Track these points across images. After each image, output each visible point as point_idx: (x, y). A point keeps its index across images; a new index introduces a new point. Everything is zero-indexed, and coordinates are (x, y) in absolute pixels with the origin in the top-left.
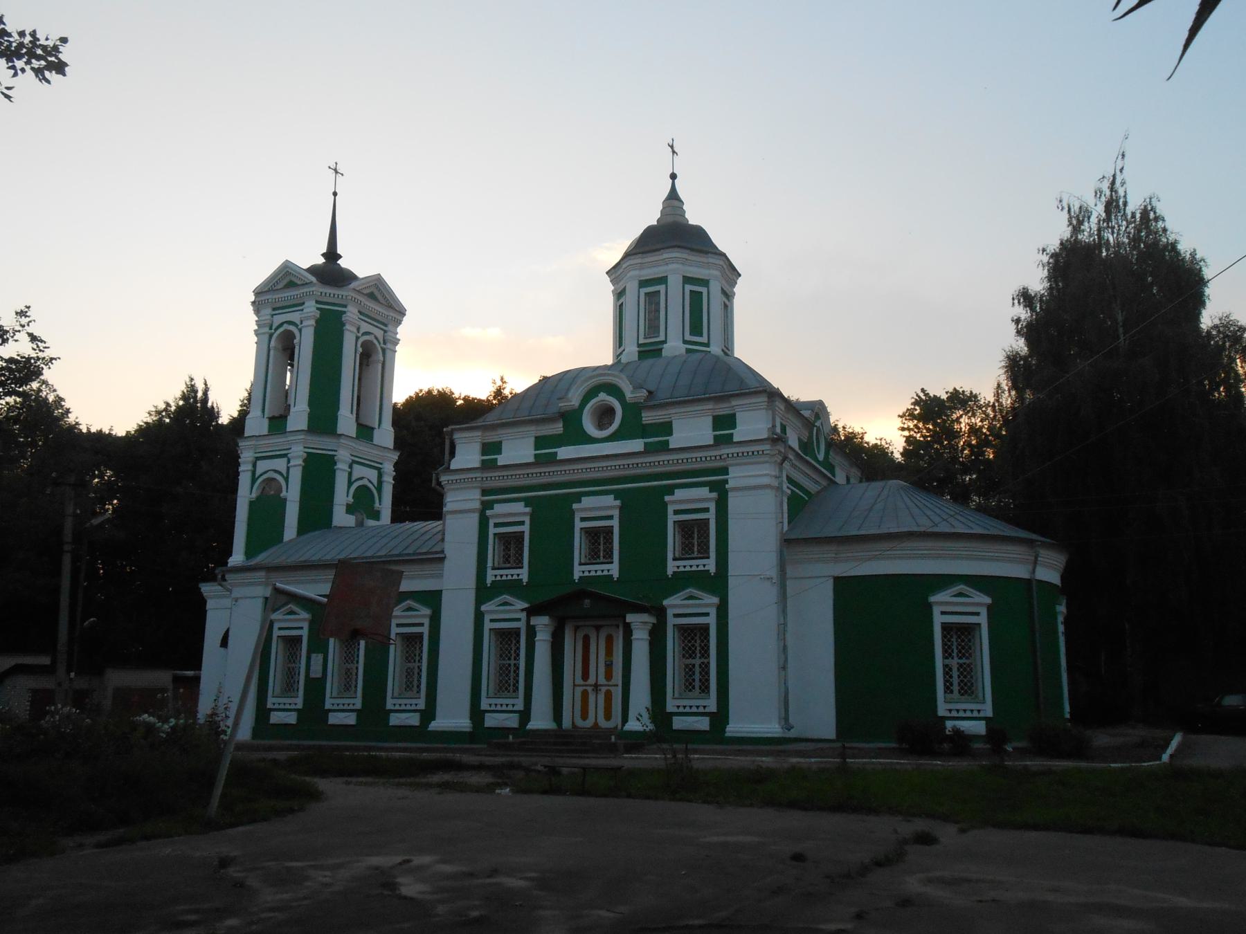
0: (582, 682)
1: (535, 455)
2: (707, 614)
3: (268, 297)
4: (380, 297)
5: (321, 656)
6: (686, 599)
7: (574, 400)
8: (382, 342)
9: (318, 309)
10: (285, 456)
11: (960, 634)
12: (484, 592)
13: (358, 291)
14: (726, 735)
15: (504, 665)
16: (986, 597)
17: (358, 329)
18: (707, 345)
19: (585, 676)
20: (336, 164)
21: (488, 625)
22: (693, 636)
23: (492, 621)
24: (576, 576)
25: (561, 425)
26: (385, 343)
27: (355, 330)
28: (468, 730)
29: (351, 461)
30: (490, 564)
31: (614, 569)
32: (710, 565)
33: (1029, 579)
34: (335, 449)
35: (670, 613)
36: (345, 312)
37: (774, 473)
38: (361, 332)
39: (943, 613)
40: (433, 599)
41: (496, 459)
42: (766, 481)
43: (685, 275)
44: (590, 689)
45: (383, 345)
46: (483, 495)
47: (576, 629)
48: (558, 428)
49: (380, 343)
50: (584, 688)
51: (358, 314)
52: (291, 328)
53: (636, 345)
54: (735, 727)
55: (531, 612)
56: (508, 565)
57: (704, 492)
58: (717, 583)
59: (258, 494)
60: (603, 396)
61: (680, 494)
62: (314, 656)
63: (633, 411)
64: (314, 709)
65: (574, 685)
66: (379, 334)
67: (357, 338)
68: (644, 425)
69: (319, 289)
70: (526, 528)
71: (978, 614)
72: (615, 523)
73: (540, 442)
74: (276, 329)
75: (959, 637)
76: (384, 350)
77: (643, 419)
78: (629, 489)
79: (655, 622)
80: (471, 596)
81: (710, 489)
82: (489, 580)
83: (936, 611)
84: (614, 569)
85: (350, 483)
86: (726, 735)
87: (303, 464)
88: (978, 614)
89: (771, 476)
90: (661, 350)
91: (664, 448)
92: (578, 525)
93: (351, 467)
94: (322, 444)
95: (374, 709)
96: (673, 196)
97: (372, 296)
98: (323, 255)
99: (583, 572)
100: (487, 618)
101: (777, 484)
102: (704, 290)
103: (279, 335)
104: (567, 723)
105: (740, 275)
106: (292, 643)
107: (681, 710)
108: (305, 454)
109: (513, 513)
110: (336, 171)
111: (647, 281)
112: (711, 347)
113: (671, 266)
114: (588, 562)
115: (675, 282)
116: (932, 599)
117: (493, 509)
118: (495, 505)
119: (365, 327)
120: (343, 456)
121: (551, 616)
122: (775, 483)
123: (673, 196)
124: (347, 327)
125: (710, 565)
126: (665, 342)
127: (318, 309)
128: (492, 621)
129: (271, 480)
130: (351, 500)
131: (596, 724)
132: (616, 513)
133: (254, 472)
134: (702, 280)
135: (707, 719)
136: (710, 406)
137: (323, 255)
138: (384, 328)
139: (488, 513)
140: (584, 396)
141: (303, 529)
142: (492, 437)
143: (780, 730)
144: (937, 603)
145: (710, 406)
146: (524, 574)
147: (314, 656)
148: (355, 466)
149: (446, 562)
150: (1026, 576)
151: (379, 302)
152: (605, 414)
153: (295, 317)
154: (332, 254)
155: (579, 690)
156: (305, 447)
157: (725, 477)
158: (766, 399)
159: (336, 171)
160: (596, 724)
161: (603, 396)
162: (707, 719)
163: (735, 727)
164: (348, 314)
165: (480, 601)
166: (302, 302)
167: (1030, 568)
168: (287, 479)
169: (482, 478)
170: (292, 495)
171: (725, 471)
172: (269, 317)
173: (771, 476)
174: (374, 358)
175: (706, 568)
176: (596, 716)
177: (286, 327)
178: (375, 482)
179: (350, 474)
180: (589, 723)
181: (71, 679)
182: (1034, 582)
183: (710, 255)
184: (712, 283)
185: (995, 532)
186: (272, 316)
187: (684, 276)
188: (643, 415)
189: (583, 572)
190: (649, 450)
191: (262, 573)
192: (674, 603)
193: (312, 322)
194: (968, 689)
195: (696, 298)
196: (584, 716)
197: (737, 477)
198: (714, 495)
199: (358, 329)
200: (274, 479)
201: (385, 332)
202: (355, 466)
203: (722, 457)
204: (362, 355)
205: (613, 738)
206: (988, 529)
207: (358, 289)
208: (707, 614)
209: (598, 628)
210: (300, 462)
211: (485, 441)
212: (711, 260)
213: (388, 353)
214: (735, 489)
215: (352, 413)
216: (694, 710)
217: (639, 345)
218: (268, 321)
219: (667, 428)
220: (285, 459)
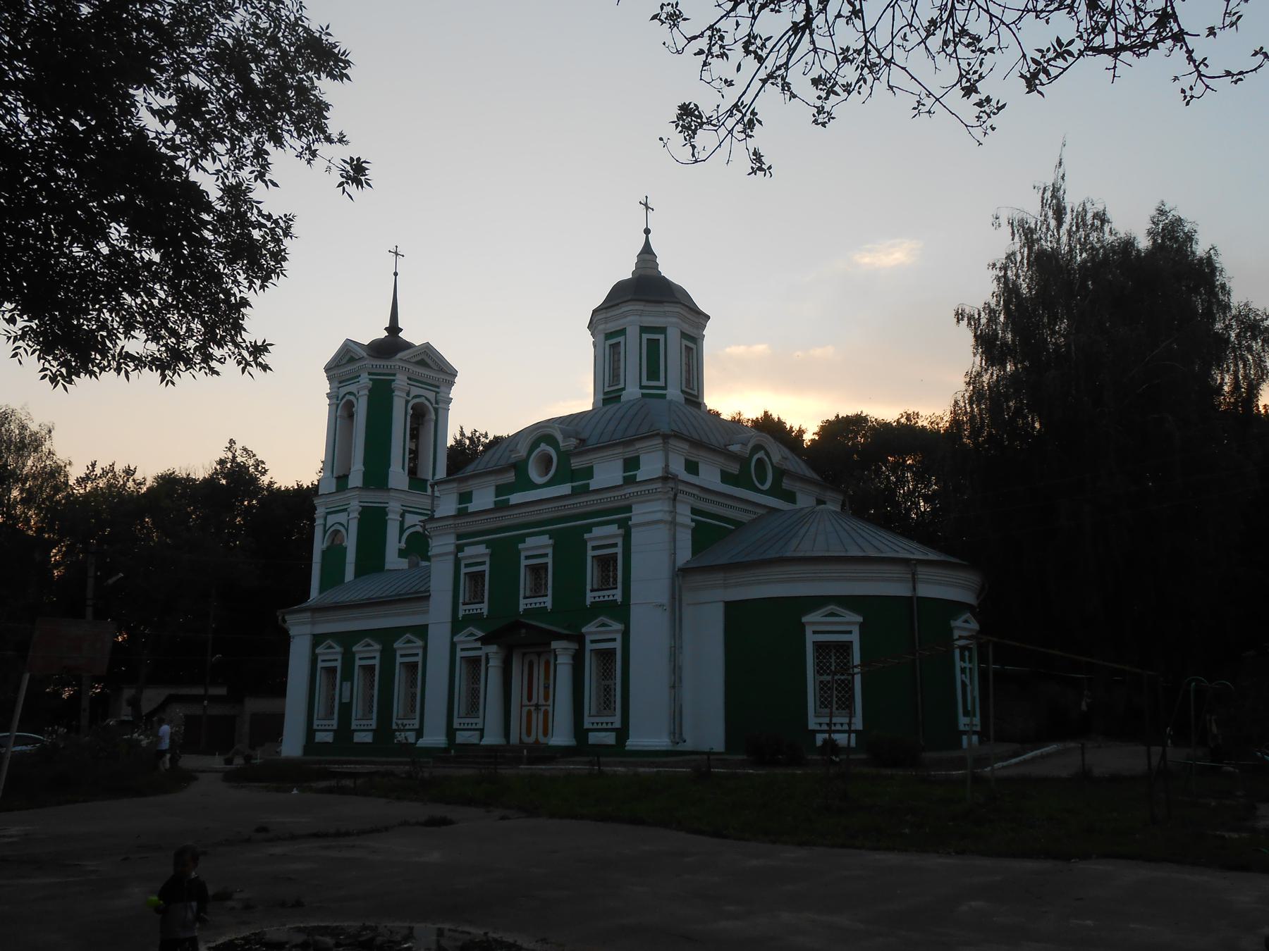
0: (527, 703)
1: (495, 501)
2: (614, 640)
3: (335, 372)
4: (429, 361)
5: (349, 684)
6: (600, 626)
7: (522, 451)
8: (433, 401)
9: (370, 379)
10: (345, 510)
11: (833, 652)
12: (457, 625)
13: (405, 360)
14: (626, 748)
16: (855, 615)
17: (408, 394)
18: (665, 388)
19: (530, 699)
20: (397, 247)
21: (459, 654)
22: (606, 656)
24: (522, 608)
25: (514, 474)
26: (437, 403)
27: (405, 395)
28: (443, 746)
30: (461, 601)
31: (548, 602)
32: (618, 595)
33: (911, 597)
34: (386, 501)
35: (588, 639)
36: (394, 380)
37: (667, 509)
38: (411, 396)
39: (815, 632)
40: (421, 631)
41: (467, 507)
42: (658, 516)
43: (641, 325)
44: (533, 708)
45: (434, 405)
46: (458, 539)
47: (524, 654)
48: (510, 477)
49: (431, 404)
50: (529, 708)
52: (352, 398)
53: (602, 393)
54: (635, 741)
55: (485, 641)
56: (476, 601)
58: (621, 611)
59: (329, 544)
60: (543, 446)
61: (597, 531)
62: (344, 683)
63: (565, 456)
64: (344, 731)
65: (522, 706)
66: (431, 396)
67: (407, 402)
68: (573, 471)
69: (370, 363)
70: (486, 568)
71: (850, 632)
72: (549, 560)
73: (500, 490)
74: (341, 400)
75: (838, 658)
76: (436, 410)
77: (572, 465)
78: (563, 528)
79: (577, 648)
80: (449, 626)
81: (618, 526)
82: (461, 614)
83: (809, 631)
84: (548, 602)
85: (402, 531)
86: (626, 748)
87: (359, 517)
88: (850, 632)
89: (665, 512)
90: (620, 396)
91: (585, 490)
92: (524, 563)
93: (402, 516)
94: (374, 498)
95: (384, 730)
96: (647, 250)
97: (422, 363)
98: (386, 329)
99: (526, 605)
101: (670, 519)
102: (661, 337)
103: (344, 404)
104: (514, 739)
105: (709, 318)
106: (331, 671)
107: (595, 726)
108: (361, 509)
109: (477, 551)
110: (397, 254)
111: (611, 333)
112: (669, 390)
113: (629, 319)
114: (532, 595)
115: (633, 332)
116: (804, 619)
117: (463, 551)
118: (465, 548)
119: (415, 391)
120: (394, 508)
121: (499, 646)
122: (668, 518)
123: (647, 250)
124: (396, 393)
125: (618, 595)
126: (624, 389)
127: (370, 379)
128: (462, 650)
129: (337, 532)
130: (403, 545)
131: (537, 739)
132: (550, 551)
133: (325, 525)
134: (659, 328)
135: (613, 735)
136: (621, 451)
137: (386, 329)
138: (436, 390)
139: (460, 555)
140: (531, 447)
141: (359, 572)
142: (465, 488)
143: (670, 744)
144: (809, 623)
145: (619, 450)
146: (484, 608)
147: (344, 683)
148: (408, 516)
149: (431, 599)
150: (909, 594)
151: (432, 368)
152: (546, 462)
153: (352, 388)
154: (394, 328)
155: (525, 709)
156: (361, 502)
157: (628, 515)
158: (661, 441)
159: (397, 254)
160: (537, 739)
161: (543, 446)
162: (613, 735)
163: (635, 741)
164: (397, 382)
165: (455, 631)
166: (358, 374)
167: (910, 585)
168: (347, 530)
169: (455, 524)
170: (351, 543)
171: (628, 509)
172: (336, 390)
173: (665, 512)
174: (427, 417)
176: (536, 735)
177: (348, 397)
179: (402, 523)
180: (532, 740)
181: (205, 707)
182: (915, 599)
183: (665, 304)
184: (669, 331)
185: (903, 555)
186: (339, 388)
187: (641, 327)
188: (572, 462)
189: (526, 605)
190: (576, 492)
191: (308, 614)
192: (590, 629)
193: (366, 392)
194: (847, 704)
195: (653, 345)
196: (529, 733)
197: (640, 513)
198: (621, 531)
199: (408, 394)
200: (339, 531)
201: (437, 393)
202: (408, 516)
204: (412, 416)
205: (525, 751)
206: (897, 552)
207: (404, 359)
208: (614, 640)
209: (539, 654)
210: (356, 515)
211: (462, 491)
212: (667, 309)
213: (441, 411)
214: (637, 525)
215: (403, 468)
216: (604, 726)
217: (605, 393)
218: (334, 394)
219: (588, 473)
220: (347, 513)
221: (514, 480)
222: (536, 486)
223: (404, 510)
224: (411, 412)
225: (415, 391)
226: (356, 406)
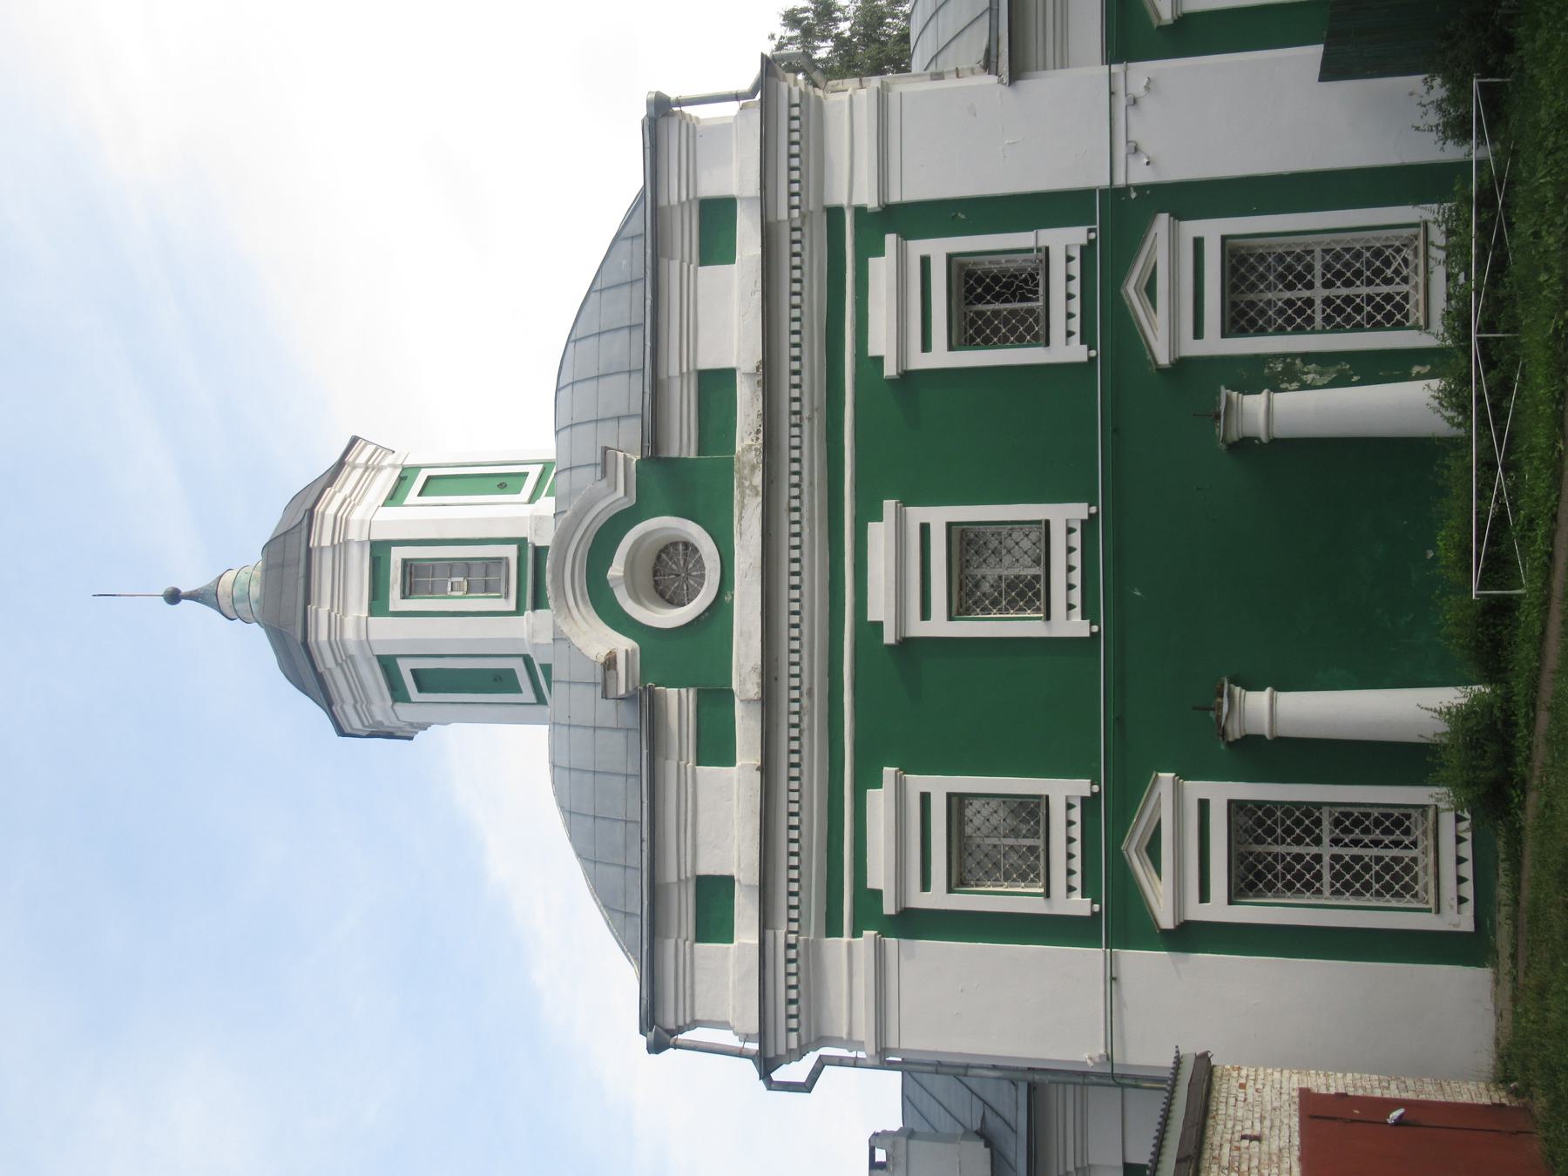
15: (1336, 876)
21: (1219, 910)
23: (1204, 896)
57: (881, 270)
82: (1079, 906)
100: (1197, 912)
128: (1204, 896)
136: (675, 265)
139: (889, 908)
145: (673, 269)
171: (835, 214)
175: (1076, 253)
188: (674, 453)
198: (891, 240)
203: (797, 224)
221: (692, 692)
222: (720, 608)
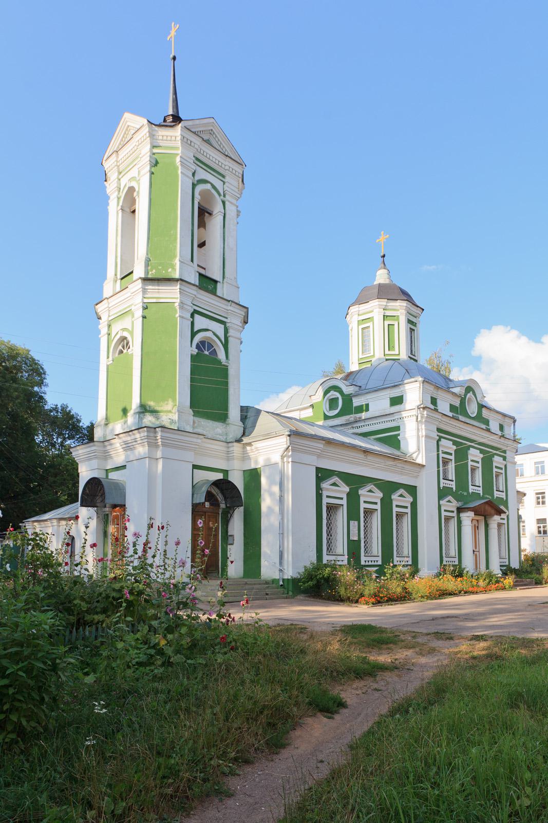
17: (194, 174)
27: (190, 175)
29: (193, 310)
51: (194, 159)
52: (134, 184)
67: (194, 186)
85: (193, 334)
93: (192, 316)
130: (195, 351)
148: (196, 316)
168: (132, 333)
178: (221, 335)
179: (192, 323)
199: (194, 174)
202: (196, 316)
223: (194, 310)
224: (199, 197)
225: (202, 174)
226: (137, 190)
